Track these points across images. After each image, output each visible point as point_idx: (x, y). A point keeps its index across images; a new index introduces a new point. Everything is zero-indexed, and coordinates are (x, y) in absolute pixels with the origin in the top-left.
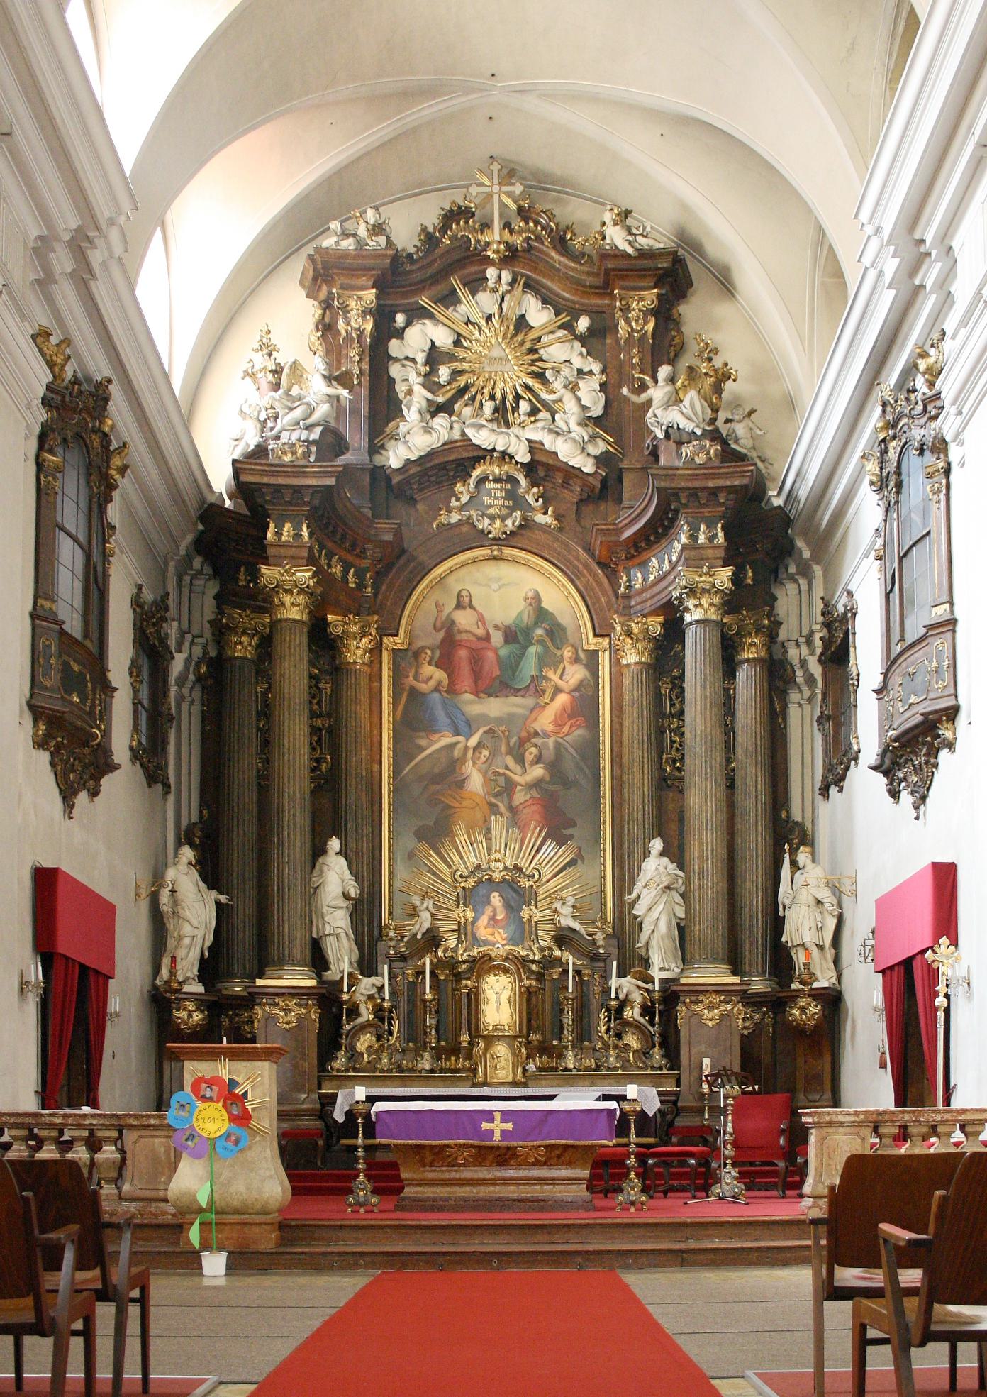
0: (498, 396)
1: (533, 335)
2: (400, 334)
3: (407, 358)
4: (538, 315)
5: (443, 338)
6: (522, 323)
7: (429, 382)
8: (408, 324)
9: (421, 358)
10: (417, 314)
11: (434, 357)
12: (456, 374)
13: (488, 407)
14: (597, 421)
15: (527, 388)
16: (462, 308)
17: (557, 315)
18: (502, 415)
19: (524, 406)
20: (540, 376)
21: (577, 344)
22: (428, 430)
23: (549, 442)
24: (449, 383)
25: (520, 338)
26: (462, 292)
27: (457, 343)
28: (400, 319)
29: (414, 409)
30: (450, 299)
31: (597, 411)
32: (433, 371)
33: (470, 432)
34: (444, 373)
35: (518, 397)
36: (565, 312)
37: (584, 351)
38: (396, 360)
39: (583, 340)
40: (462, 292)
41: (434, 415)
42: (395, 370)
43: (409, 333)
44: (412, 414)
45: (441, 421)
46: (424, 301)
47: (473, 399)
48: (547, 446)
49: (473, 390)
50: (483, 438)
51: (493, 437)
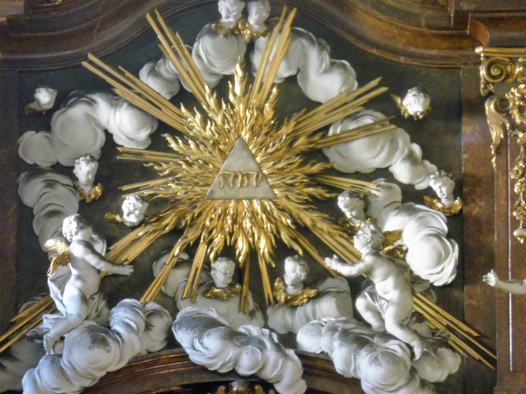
0: (242, 247)
1: (317, 120)
2: (43, 121)
3: (57, 168)
4: (327, 83)
5: (124, 125)
6: (292, 98)
7: (98, 216)
8: (62, 102)
9: (84, 170)
10: (77, 86)
11: (116, 168)
12: (156, 207)
13: (222, 271)
14: (444, 295)
15: (302, 229)
16: (169, 66)
17: (362, 81)
18: (251, 281)
19: (292, 269)
20: (326, 206)
21: (402, 137)
22: (101, 333)
23: (340, 356)
24: (142, 223)
25: (285, 130)
26: (166, 40)
27: (156, 142)
28: (44, 97)
29: (72, 289)
30: (140, 52)
31: (444, 274)
32: (111, 196)
33: (183, 337)
34: (131, 208)
35: (281, 251)
36: (380, 74)
37: (417, 149)
38: (35, 171)
39: (414, 127)
40: (166, 40)
41: (112, 301)
42: (32, 193)
43: (58, 121)
44: (68, 297)
45: (122, 316)
46: (94, 65)
47: (191, 250)
48: (339, 366)
49: (190, 236)
50: (206, 350)
51: (231, 353)
